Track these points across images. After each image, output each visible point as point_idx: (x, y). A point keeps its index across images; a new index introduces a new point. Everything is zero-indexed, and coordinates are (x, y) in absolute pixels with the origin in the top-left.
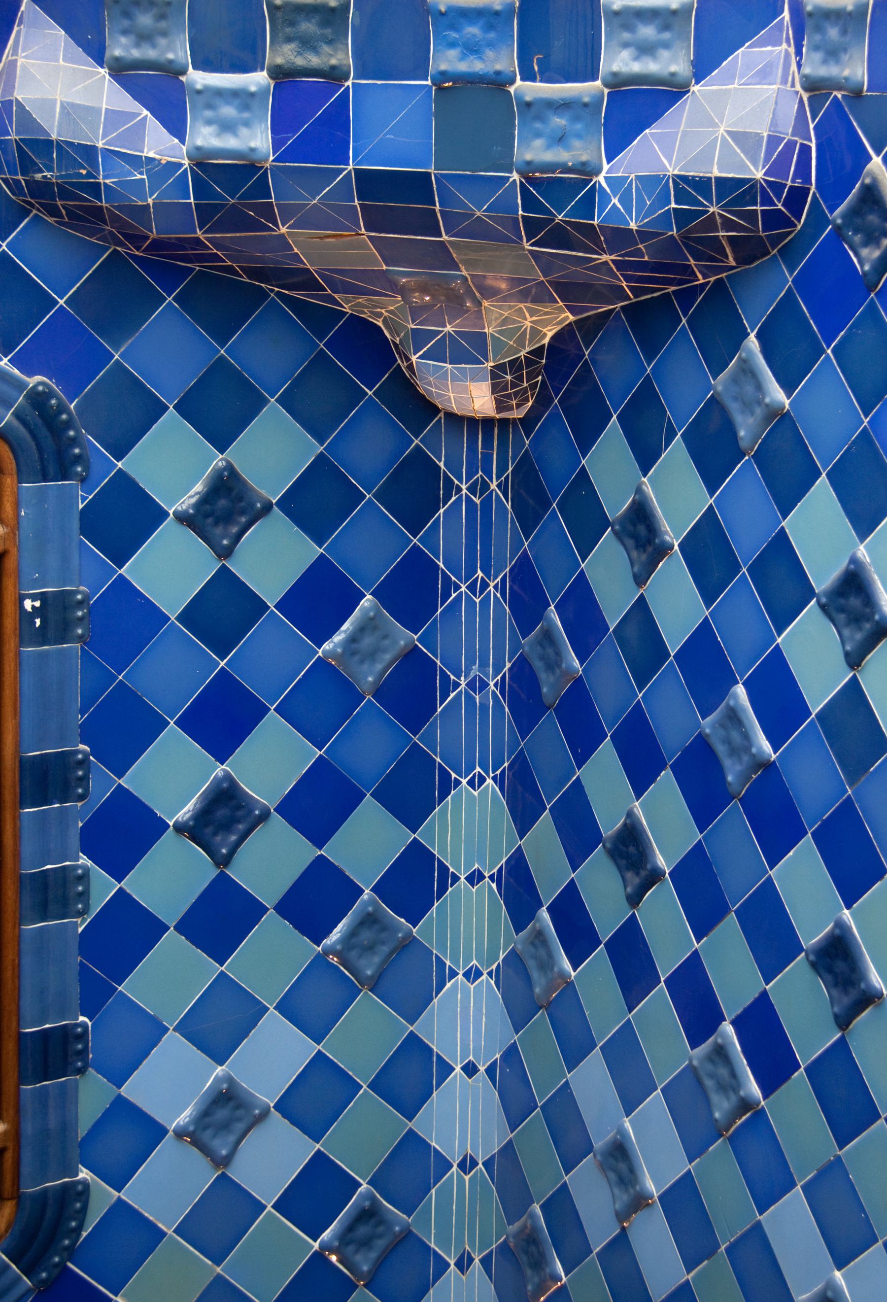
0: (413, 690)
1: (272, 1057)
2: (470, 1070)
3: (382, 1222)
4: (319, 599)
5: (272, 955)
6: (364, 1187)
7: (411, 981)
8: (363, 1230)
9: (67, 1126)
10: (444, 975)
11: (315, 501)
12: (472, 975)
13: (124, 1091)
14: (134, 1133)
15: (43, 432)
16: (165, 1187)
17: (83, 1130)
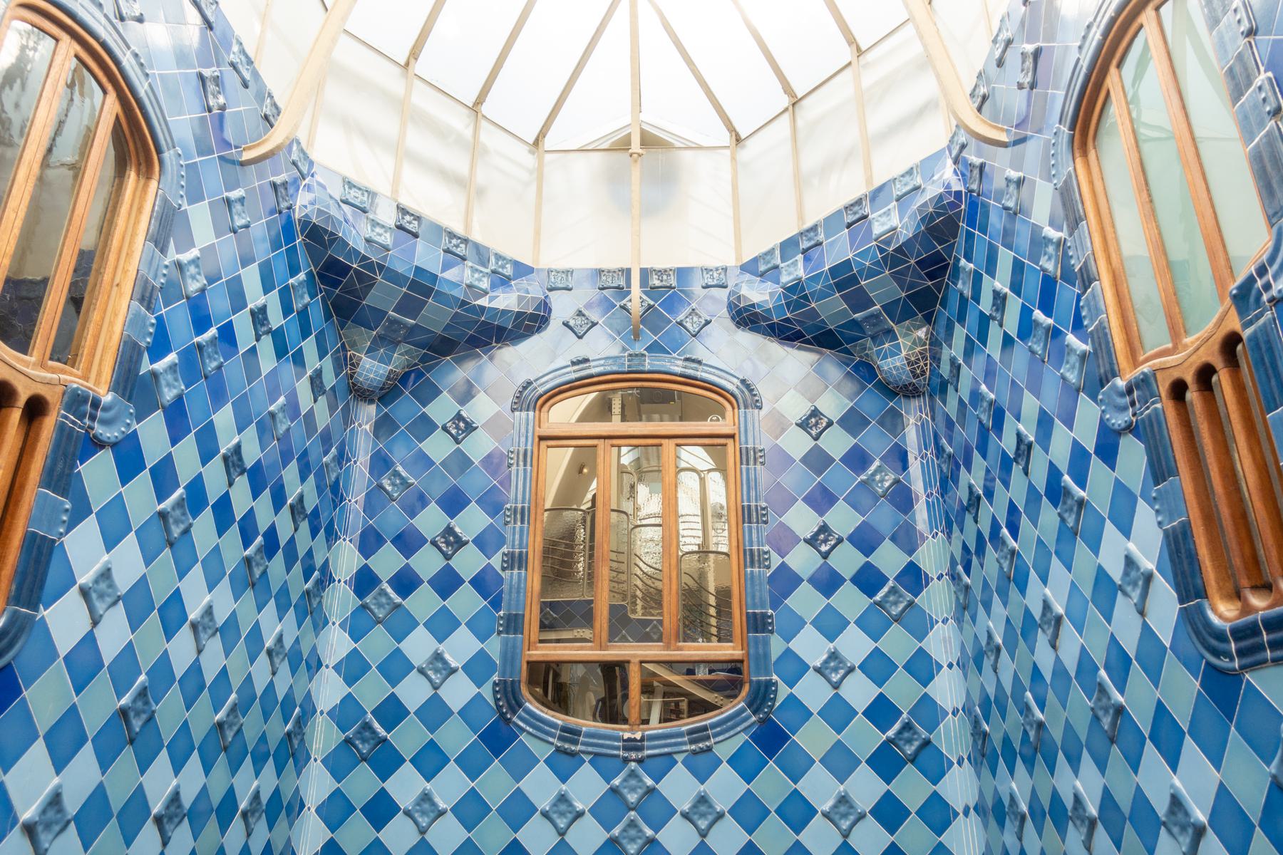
0: (902, 498)
1: (855, 645)
2: (950, 666)
3: (915, 733)
4: (857, 459)
5: (850, 601)
6: (905, 715)
7: (920, 626)
8: (906, 735)
9: (767, 655)
10: (933, 623)
11: (853, 421)
12: (945, 621)
13: (790, 645)
14: (795, 668)
15: (746, 392)
16: (812, 691)
17: (774, 657)
